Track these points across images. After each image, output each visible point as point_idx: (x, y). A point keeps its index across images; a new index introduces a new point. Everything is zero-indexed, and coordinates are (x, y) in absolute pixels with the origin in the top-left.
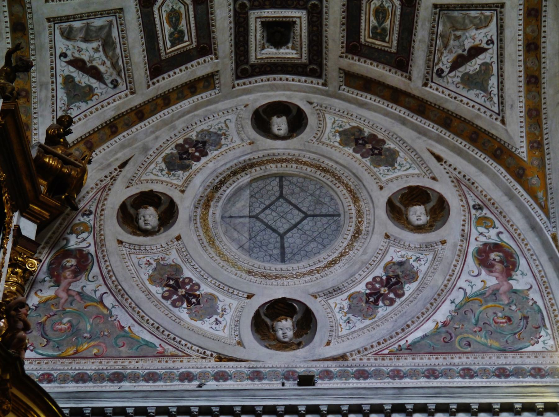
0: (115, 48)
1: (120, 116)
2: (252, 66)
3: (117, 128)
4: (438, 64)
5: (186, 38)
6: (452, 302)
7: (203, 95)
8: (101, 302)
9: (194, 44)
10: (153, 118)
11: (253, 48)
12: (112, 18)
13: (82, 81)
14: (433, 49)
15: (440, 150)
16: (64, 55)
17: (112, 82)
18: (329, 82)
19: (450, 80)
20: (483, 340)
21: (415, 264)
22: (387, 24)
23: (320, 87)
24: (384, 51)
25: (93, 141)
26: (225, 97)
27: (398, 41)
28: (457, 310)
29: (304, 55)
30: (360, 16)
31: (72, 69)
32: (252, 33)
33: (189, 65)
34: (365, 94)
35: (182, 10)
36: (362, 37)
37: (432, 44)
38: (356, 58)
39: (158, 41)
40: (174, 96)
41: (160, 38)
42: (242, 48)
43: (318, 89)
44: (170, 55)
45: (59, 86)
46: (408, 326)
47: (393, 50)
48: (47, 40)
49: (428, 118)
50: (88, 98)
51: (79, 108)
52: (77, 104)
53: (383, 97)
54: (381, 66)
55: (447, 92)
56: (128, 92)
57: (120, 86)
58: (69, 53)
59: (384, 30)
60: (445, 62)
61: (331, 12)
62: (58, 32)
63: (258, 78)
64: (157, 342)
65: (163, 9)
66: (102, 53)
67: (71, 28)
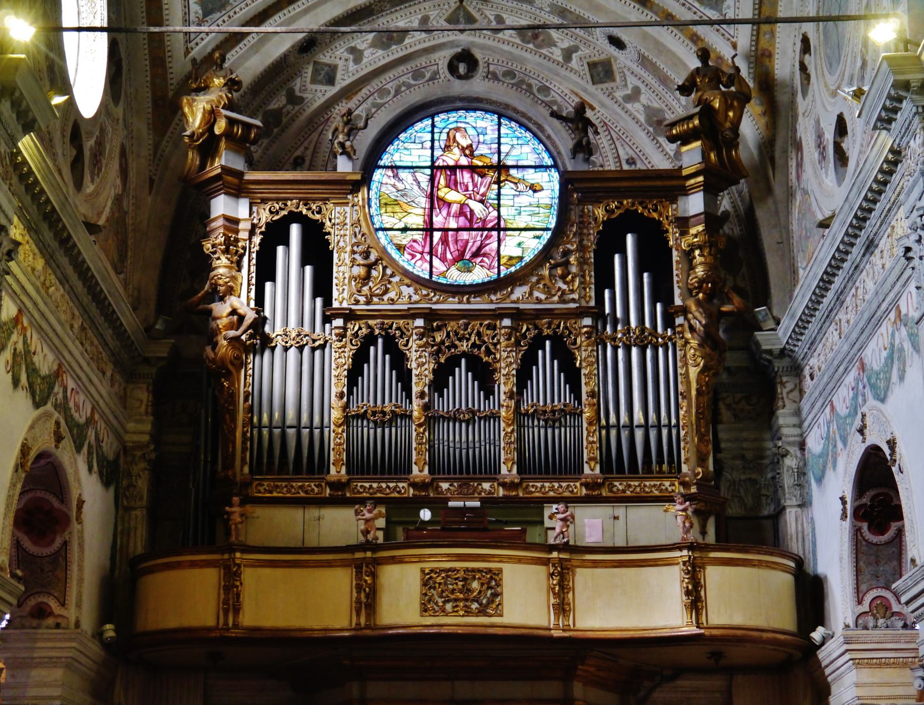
45: (702, 9)
51: (729, 7)
52: (724, 6)
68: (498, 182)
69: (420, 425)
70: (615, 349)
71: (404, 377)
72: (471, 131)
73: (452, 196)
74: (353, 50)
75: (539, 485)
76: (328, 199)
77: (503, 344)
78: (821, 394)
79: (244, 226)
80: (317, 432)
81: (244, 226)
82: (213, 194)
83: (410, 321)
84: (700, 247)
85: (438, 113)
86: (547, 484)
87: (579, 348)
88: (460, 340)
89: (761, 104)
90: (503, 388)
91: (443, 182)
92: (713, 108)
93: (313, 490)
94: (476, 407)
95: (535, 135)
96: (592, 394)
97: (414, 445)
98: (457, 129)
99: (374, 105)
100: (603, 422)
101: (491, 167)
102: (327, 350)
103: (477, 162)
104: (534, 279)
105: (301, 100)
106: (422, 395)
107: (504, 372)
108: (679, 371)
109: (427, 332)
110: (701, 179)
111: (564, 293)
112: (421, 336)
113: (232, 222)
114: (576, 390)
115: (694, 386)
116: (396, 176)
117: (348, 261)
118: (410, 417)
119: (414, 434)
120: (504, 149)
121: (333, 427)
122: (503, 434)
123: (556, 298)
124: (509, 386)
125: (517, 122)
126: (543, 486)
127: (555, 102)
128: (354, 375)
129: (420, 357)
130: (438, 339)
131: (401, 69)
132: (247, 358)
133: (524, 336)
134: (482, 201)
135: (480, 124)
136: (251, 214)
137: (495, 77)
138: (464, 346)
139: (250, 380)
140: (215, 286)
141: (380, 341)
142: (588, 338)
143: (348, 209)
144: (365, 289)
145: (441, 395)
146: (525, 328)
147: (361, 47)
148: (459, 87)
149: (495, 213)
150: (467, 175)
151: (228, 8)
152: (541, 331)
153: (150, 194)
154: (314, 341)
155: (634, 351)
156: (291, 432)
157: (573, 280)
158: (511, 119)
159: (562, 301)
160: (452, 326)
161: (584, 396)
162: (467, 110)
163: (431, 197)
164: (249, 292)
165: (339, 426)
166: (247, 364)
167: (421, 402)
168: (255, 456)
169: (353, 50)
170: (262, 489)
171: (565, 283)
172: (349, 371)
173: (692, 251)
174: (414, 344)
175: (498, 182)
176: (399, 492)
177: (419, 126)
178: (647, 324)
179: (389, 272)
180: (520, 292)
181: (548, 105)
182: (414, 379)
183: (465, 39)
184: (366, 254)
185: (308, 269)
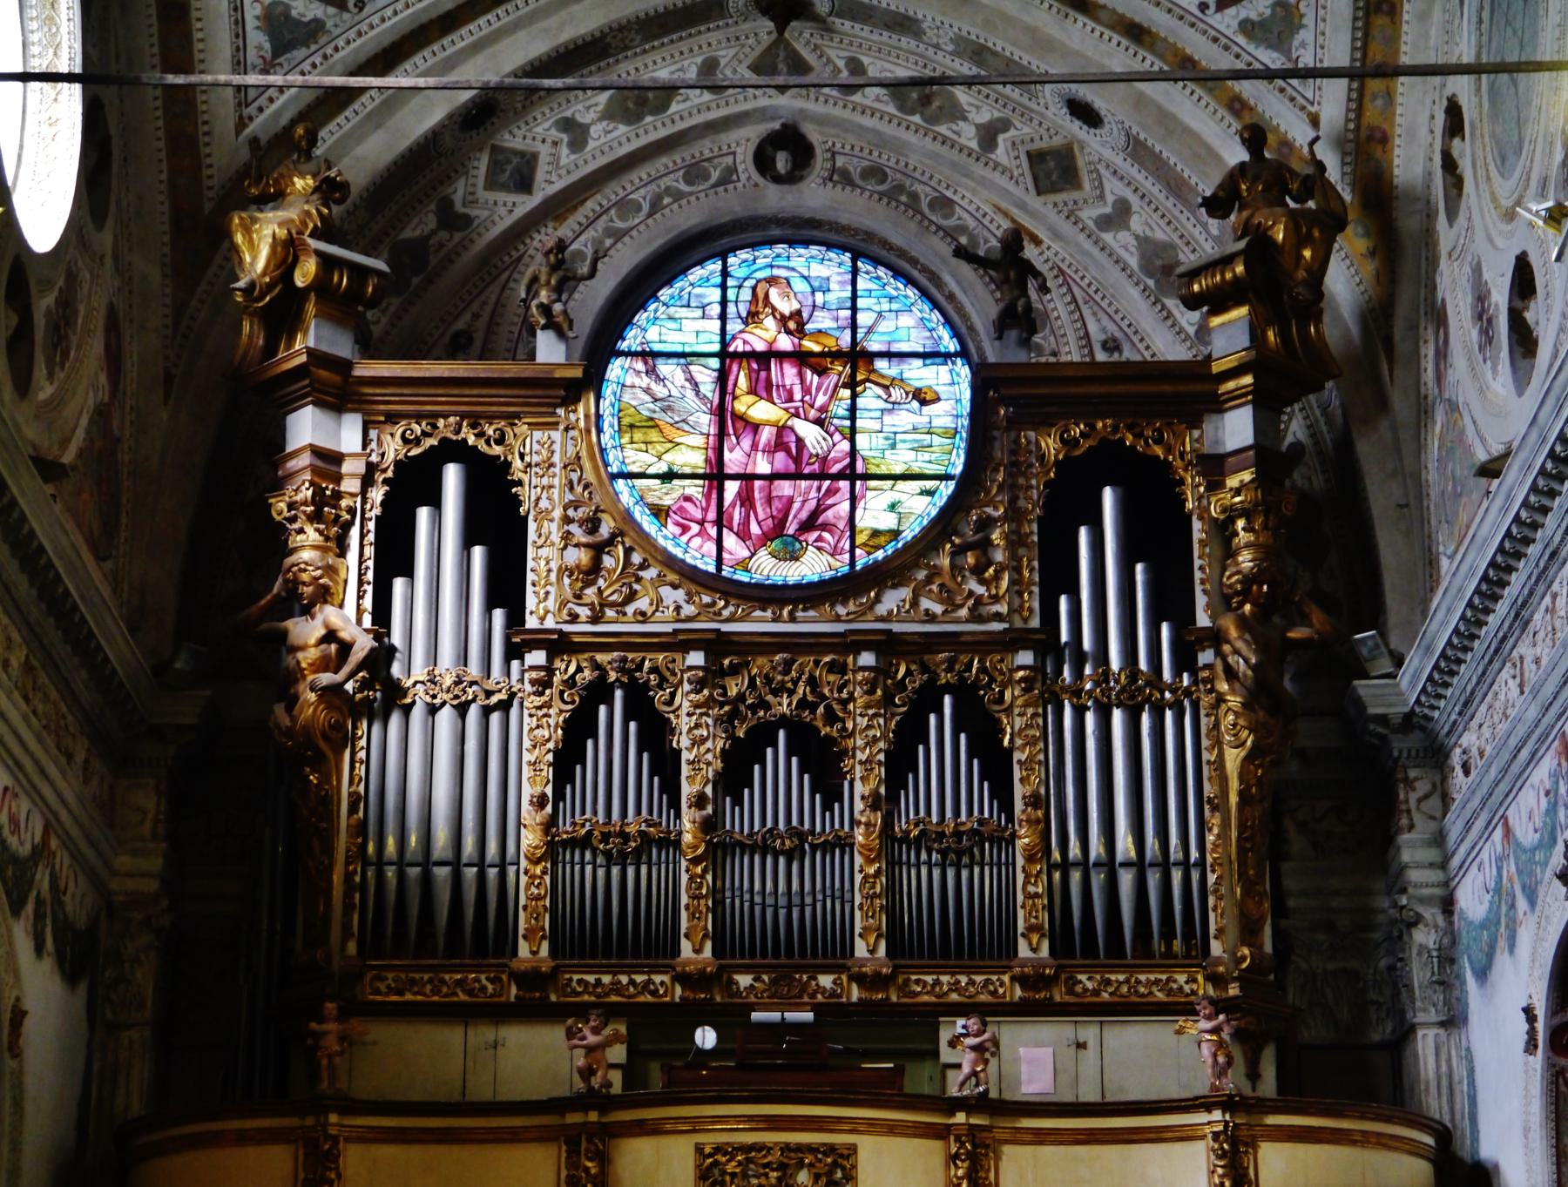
13: (1261, 9)
31: (1231, 11)
45: (1251, 48)
50: (1296, 21)
51: (1303, 45)
52: (1296, 43)
68: (852, 384)
69: (695, 861)
71: (666, 766)
72: (800, 286)
73: (762, 411)
74: (568, 125)
75: (929, 979)
76: (518, 416)
77: (860, 702)
78: (1484, 803)
79: (352, 468)
80: (492, 873)
81: (352, 468)
82: (293, 404)
83: (678, 656)
84: (1246, 513)
85: (734, 249)
86: (945, 979)
87: (1009, 710)
88: (776, 693)
89: (1367, 235)
90: (859, 788)
91: (743, 382)
92: (1273, 241)
93: (484, 988)
94: (807, 826)
95: (924, 293)
96: (1035, 801)
97: (684, 899)
98: (772, 281)
100: (1056, 856)
101: (837, 355)
102: (514, 712)
103: (810, 345)
104: (921, 575)
105: (467, 220)
106: (700, 801)
107: (861, 756)
108: (1206, 756)
109: (711, 677)
110: (1248, 380)
111: (979, 601)
113: (328, 461)
115: (1234, 785)
116: (651, 372)
117: (556, 537)
118: (677, 844)
119: (685, 878)
120: (864, 319)
121: (524, 863)
122: (858, 878)
123: (964, 612)
124: (873, 784)
125: (888, 266)
126: (937, 982)
127: (963, 229)
128: (567, 760)
129: (697, 726)
130: (733, 691)
131: (664, 161)
132: (355, 727)
133: (901, 686)
134: (819, 422)
135: (818, 270)
136: (366, 442)
137: (846, 179)
138: (784, 705)
139: (361, 770)
140: (293, 585)
141: (618, 694)
142: (1026, 691)
143: (556, 435)
144: (590, 592)
145: (738, 801)
147: (585, 118)
148: (775, 199)
149: (845, 446)
150: (790, 372)
151: (323, 40)
152: (934, 677)
153: (166, 403)
154: (489, 694)
155: (1117, 716)
156: (442, 873)
157: (997, 577)
158: (876, 261)
159: (975, 617)
160: (759, 665)
161: (1019, 805)
162: (792, 243)
163: (721, 412)
164: (360, 597)
165: (537, 862)
166: (355, 738)
167: (698, 815)
169: (568, 125)
170: (383, 988)
171: (982, 582)
172: (556, 752)
173: (1231, 520)
174: (684, 702)
175: (852, 384)
176: (654, 993)
177: (697, 273)
178: (1143, 665)
179: (636, 558)
180: (893, 600)
181: (949, 234)
182: (685, 770)
183: (788, 103)
184: (592, 524)
185: (478, 552)
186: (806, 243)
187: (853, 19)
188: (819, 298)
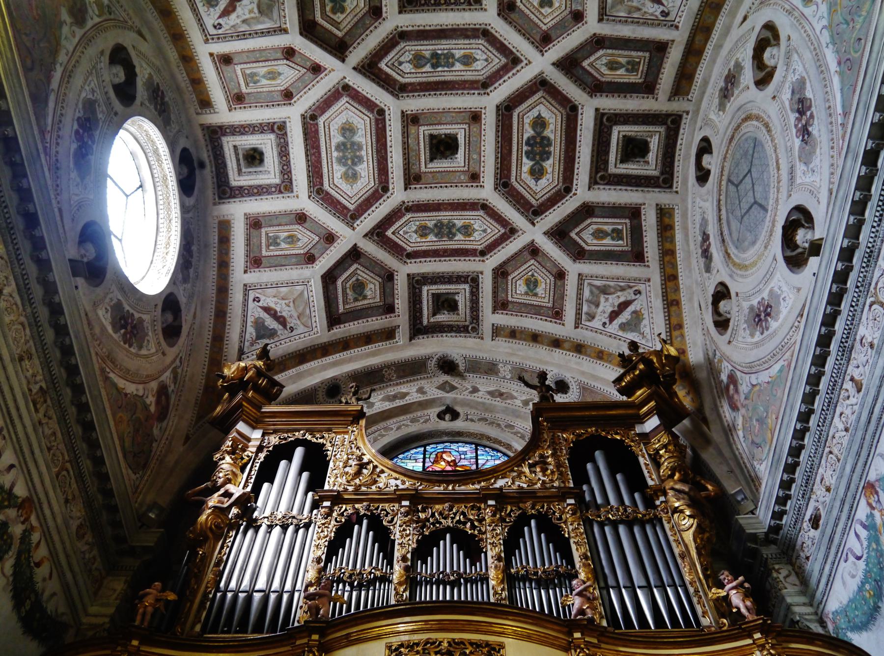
0: (609, 286)
1: (665, 295)
2: (662, 173)
3: (674, 300)
4: (656, 16)
5: (620, 227)
6: (827, 47)
7: (676, 220)
8: (753, 386)
9: (627, 221)
10: (679, 267)
11: (645, 172)
12: (586, 282)
14: (641, 21)
15: (739, 18)
16: (604, 324)
17: (635, 294)
18: (687, 109)
19: (671, 5)
20: (861, 20)
21: (797, 77)
22: (623, 60)
23: (689, 116)
24: (649, 62)
25: (675, 323)
26: (684, 200)
27: (638, 51)
28: (834, 44)
29: (657, 129)
30: (617, 83)
31: (615, 322)
32: (630, 172)
33: (644, 228)
34: (696, 79)
35: (595, 227)
36: (637, 81)
37: (636, 22)
38: (658, 86)
39: (614, 251)
40: (668, 246)
41: (613, 248)
42: (643, 181)
43: (691, 119)
44: (629, 243)
46: (830, 107)
47: (647, 55)
48: (590, 333)
49: (713, 24)
51: (645, 326)
53: (698, 63)
54: (664, 65)
55: (682, 8)
56: (647, 284)
57: (641, 289)
58: (604, 320)
59: (628, 63)
60: (654, 9)
61: (614, 107)
62: (588, 323)
63: (676, 169)
64: (781, 363)
65: (589, 241)
66: (610, 296)
67: (587, 314)
69: (400, 584)
70: (602, 525)
77: (488, 521)
80: (285, 597)
84: (665, 446)
85: (429, 445)
87: (565, 522)
88: (445, 518)
89: (684, 388)
90: (490, 554)
94: (462, 570)
99: (379, 435)
102: (311, 529)
106: (404, 559)
107: (489, 541)
108: (671, 539)
109: (412, 511)
110: (652, 404)
111: (544, 482)
112: (407, 514)
114: (568, 556)
118: (390, 582)
120: (480, 462)
122: (491, 592)
125: (489, 447)
127: (519, 433)
128: (334, 547)
129: (404, 530)
130: (422, 516)
132: (228, 532)
137: (472, 420)
138: (449, 523)
143: (346, 436)
144: (357, 481)
145: (425, 562)
146: (509, 508)
148: (446, 425)
151: (276, 339)
153: (184, 444)
156: (257, 596)
158: (485, 446)
160: (438, 507)
162: (452, 442)
167: (403, 565)
168: (212, 618)
171: (544, 475)
172: (330, 542)
174: (398, 520)
180: (500, 483)
181: (515, 434)
182: (397, 547)
186: (457, 442)
187: (474, 372)
188: (463, 456)
